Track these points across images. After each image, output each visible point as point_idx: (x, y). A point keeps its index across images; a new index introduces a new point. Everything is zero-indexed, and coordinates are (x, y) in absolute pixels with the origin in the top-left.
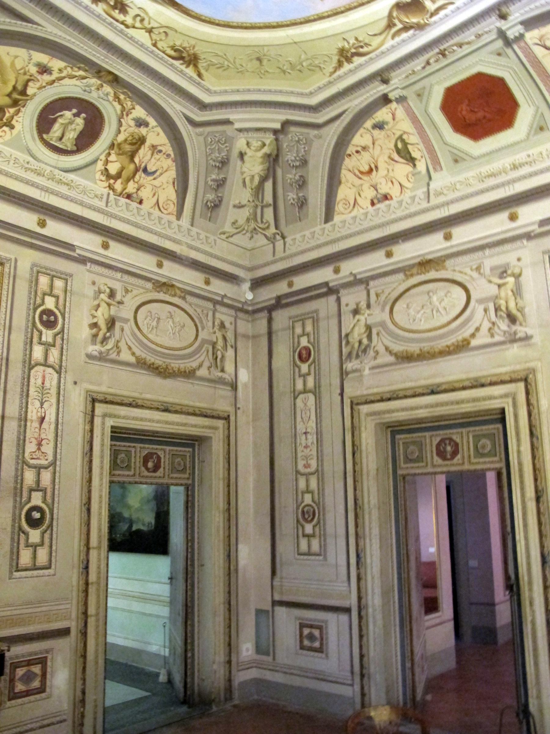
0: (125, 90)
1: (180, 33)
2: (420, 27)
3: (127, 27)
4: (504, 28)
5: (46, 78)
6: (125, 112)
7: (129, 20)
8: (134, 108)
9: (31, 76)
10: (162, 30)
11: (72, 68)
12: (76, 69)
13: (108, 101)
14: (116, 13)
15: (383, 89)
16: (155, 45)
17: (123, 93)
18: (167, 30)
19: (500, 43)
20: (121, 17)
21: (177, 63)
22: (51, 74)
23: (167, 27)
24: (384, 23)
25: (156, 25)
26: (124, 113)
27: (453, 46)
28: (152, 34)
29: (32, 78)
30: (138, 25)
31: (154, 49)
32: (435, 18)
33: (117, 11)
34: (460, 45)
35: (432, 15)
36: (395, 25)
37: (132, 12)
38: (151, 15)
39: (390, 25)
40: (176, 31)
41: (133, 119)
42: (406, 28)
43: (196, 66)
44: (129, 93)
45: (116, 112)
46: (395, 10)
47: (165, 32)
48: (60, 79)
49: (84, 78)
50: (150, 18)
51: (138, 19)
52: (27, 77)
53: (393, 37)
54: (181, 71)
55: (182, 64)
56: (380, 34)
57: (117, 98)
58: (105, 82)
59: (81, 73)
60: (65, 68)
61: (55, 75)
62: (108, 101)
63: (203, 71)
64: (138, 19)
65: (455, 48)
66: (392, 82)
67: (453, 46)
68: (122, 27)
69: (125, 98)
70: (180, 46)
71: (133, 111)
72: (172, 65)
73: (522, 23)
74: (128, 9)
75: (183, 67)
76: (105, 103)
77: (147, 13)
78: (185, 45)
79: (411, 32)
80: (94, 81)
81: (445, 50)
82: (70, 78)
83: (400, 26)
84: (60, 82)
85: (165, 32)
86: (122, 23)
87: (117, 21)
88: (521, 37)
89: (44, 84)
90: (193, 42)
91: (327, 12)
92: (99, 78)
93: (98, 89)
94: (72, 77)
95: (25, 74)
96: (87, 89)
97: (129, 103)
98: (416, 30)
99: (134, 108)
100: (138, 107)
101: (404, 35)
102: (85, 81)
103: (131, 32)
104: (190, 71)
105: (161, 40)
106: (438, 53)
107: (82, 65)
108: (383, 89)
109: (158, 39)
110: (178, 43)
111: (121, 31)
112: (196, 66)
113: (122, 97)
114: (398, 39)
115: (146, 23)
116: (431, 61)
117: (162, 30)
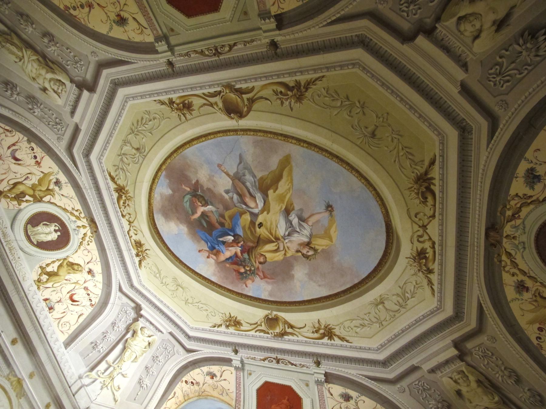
0: (498, 214)
1: (407, 206)
2: (229, 86)
3: (434, 243)
4: (169, 53)
5: (529, 283)
6: (527, 201)
7: (427, 245)
8: (517, 195)
9: (536, 296)
10: (416, 220)
11: (504, 267)
12: (503, 263)
13: (523, 222)
14: (430, 254)
15: (280, 37)
16: (433, 216)
17: (503, 213)
18: (413, 216)
19: (173, 40)
20: (430, 251)
21: (436, 189)
22: (522, 281)
23: (410, 218)
24: (256, 106)
25: (416, 228)
26: (529, 201)
27: (208, 56)
28: (425, 224)
29: (537, 295)
30: (426, 237)
31: (437, 214)
32: (219, 89)
33: (427, 255)
34: (202, 53)
35: (220, 93)
36: (248, 99)
37: (420, 246)
38: (411, 234)
39: (252, 101)
40: (408, 210)
41: (532, 188)
42: (240, 92)
43: (426, 173)
44: (499, 209)
45: (534, 209)
46: (244, 113)
47: (416, 217)
48: (524, 273)
49: (509, 255)
50: (414, 233)
51: (421, 239)
52: (538, 299)
53: (253, 88)
54: (442, 180)
55: (435, 185)
56: (261, 98)
57: (513, 217)
58: (502, 236)
59: (504, 258)
60: (508, 272)
61: (521, 277)
62: (523, 222)
63: (427, 163)
64: (421, 239)
65: (207, 53)
66: (268, 40)
67: (208, 56)
68: (436, 246)
69: (509, 209)
70: (418, 198)
71: (520, 194)
72: (442, 192)
73: (157, 52)
74: (419, 250)
75: (436, 182)
76: (528, 223)
77: (412, 237)
78: (413, 195)
79: (238, 86)
80: (507, 244)
81: (215, 55)
82: (517, 265)
83: (245, 96)
84: (527, 272)
85: (416, 217)
86: (433, 247)
87: (434, 252)
88: (158, 39)
89: (538, 284)
90: (407, 193)
91: (291, 143)
92: (500, 243)
93: (514, 238)
94: (515, 265)
95: (536, 301)
96: (520, 247)
97: (513, 203)
98: (234, 86)
99: (517, 195)
100: (512, 192)
101: (244, 86)
102: (513, 252)
103: (436, 239)
104: (435, 173)
105: (425, 215)
106: (220, 54)
107: (496, 260)
108: (280, 37)
109: (426, 217)
110: (417, 201)
111: (441, 245)
112: (426, 173)
113: (509, 213)
114: (250, 85)
115: (419, 233)
116: (227, 49)
117: (416, 220)
